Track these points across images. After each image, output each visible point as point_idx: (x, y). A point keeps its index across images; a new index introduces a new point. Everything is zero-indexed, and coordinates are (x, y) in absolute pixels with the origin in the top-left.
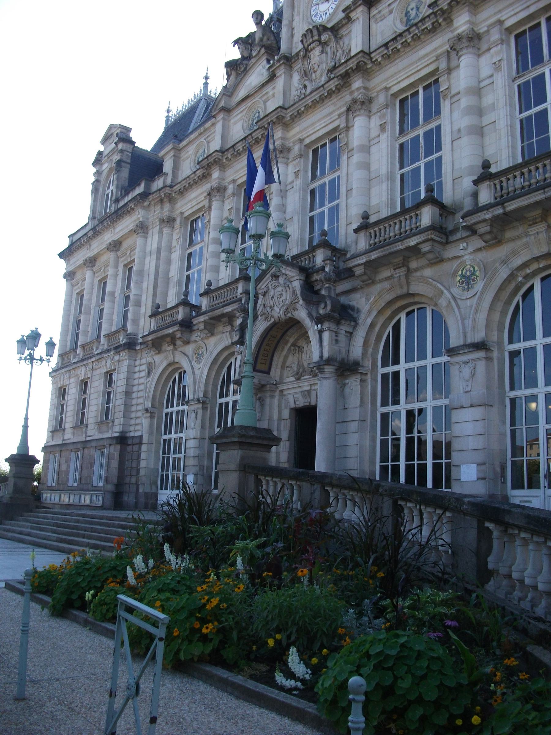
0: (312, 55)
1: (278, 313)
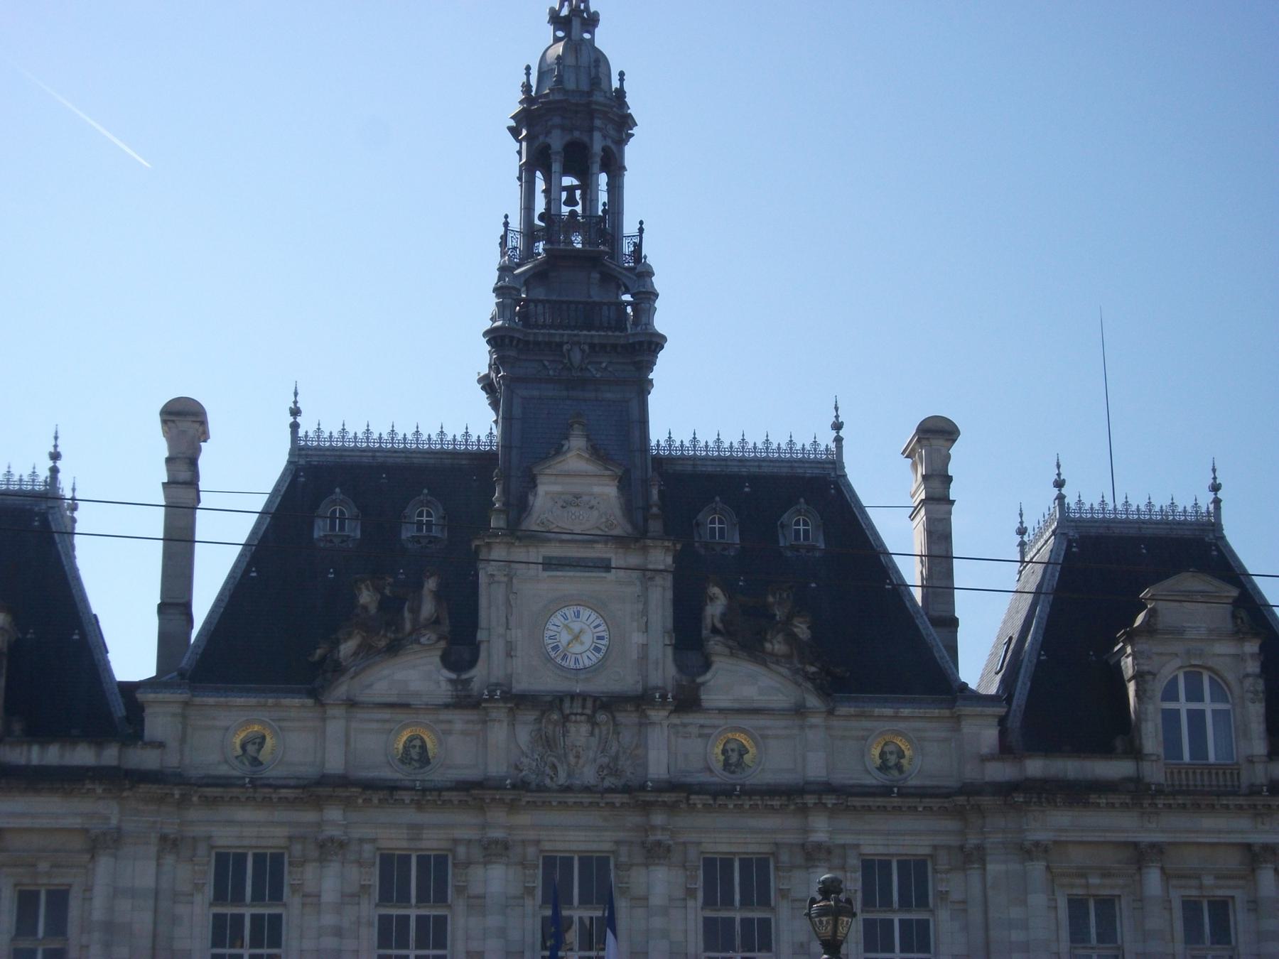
0: (572, 728)
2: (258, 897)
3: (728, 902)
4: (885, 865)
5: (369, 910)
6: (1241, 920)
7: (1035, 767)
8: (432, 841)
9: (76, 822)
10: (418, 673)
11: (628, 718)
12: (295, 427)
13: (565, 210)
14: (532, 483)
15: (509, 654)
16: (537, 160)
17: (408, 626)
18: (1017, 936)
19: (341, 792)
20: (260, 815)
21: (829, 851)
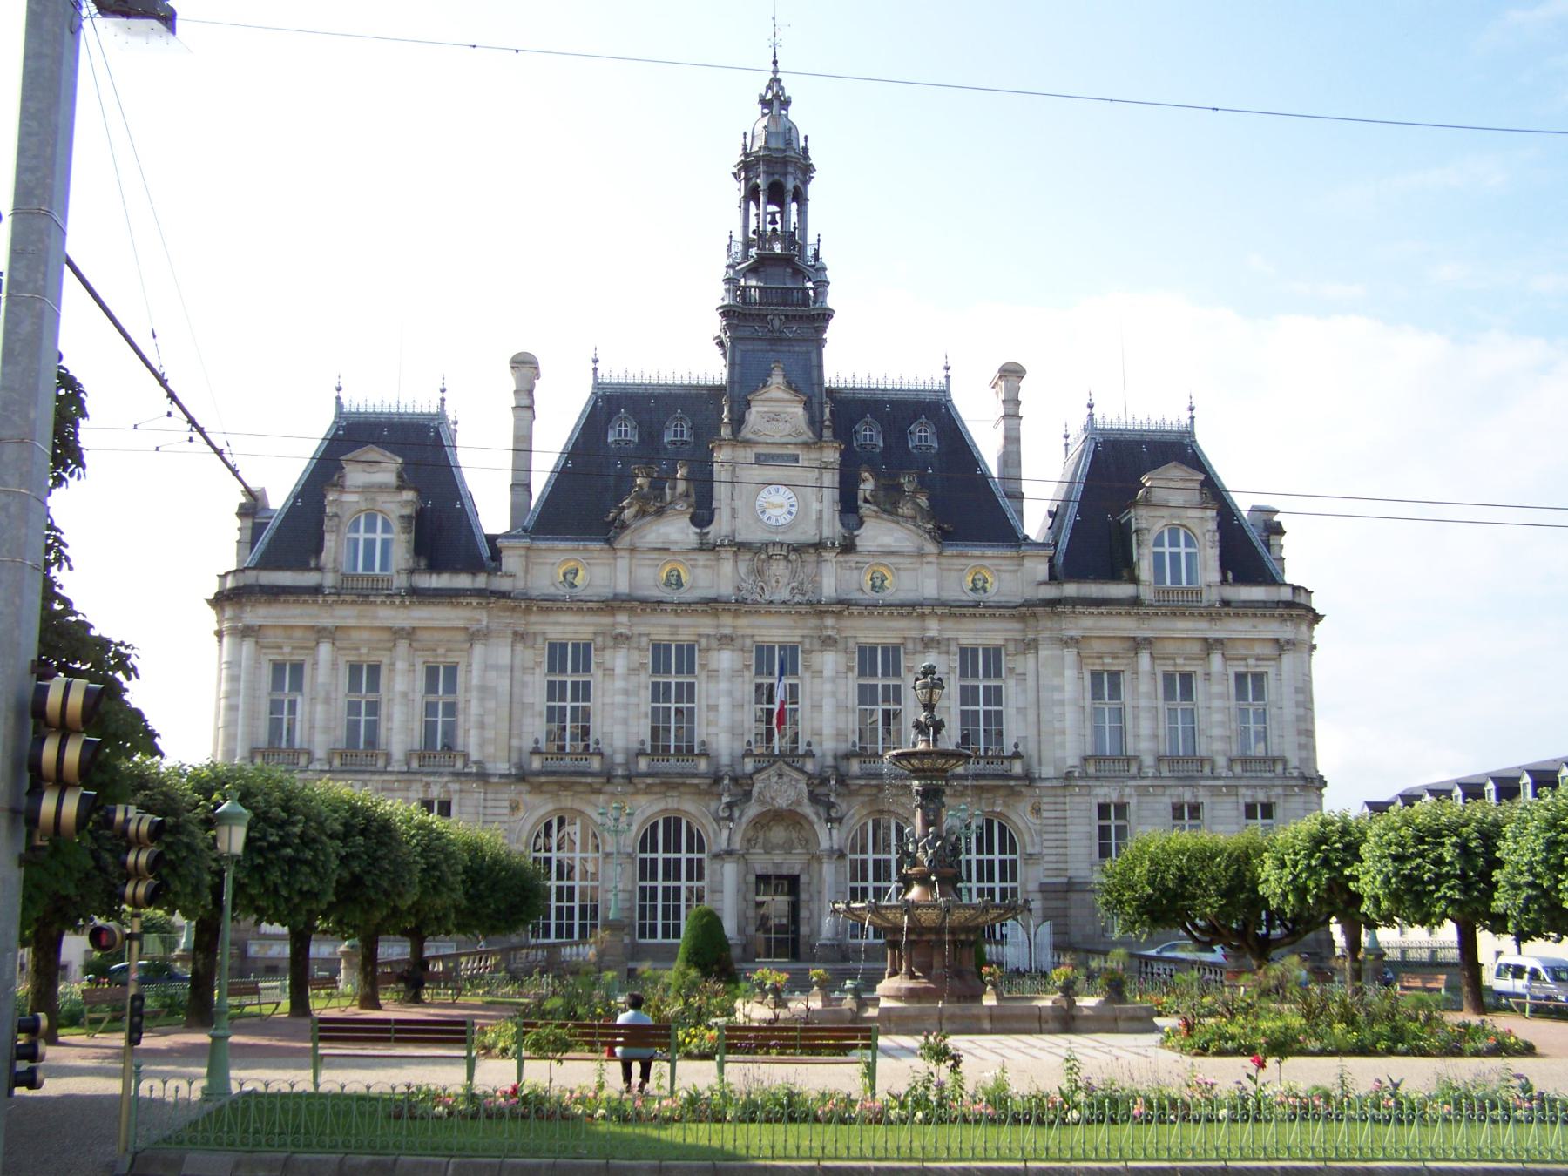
0: (774, 564)
1: (782, 803)
2: (575, 670)
3: (874, 674)
4: (974, 651)
5: (646, 679)
6: (1198, 685)
7: (1071, 589)
8: (685, 636)
9: (461, 624)
10: (676, 529)
11: (810, 557)
12: (595, 370)
13: (769, 227)
14: (748, 406)
15: (734, 517)
16: (752, 194)
17: (668, 498)
18: (1057, 696)
19: (629, 605)
20: (576, 619)
21: (939, 642)
